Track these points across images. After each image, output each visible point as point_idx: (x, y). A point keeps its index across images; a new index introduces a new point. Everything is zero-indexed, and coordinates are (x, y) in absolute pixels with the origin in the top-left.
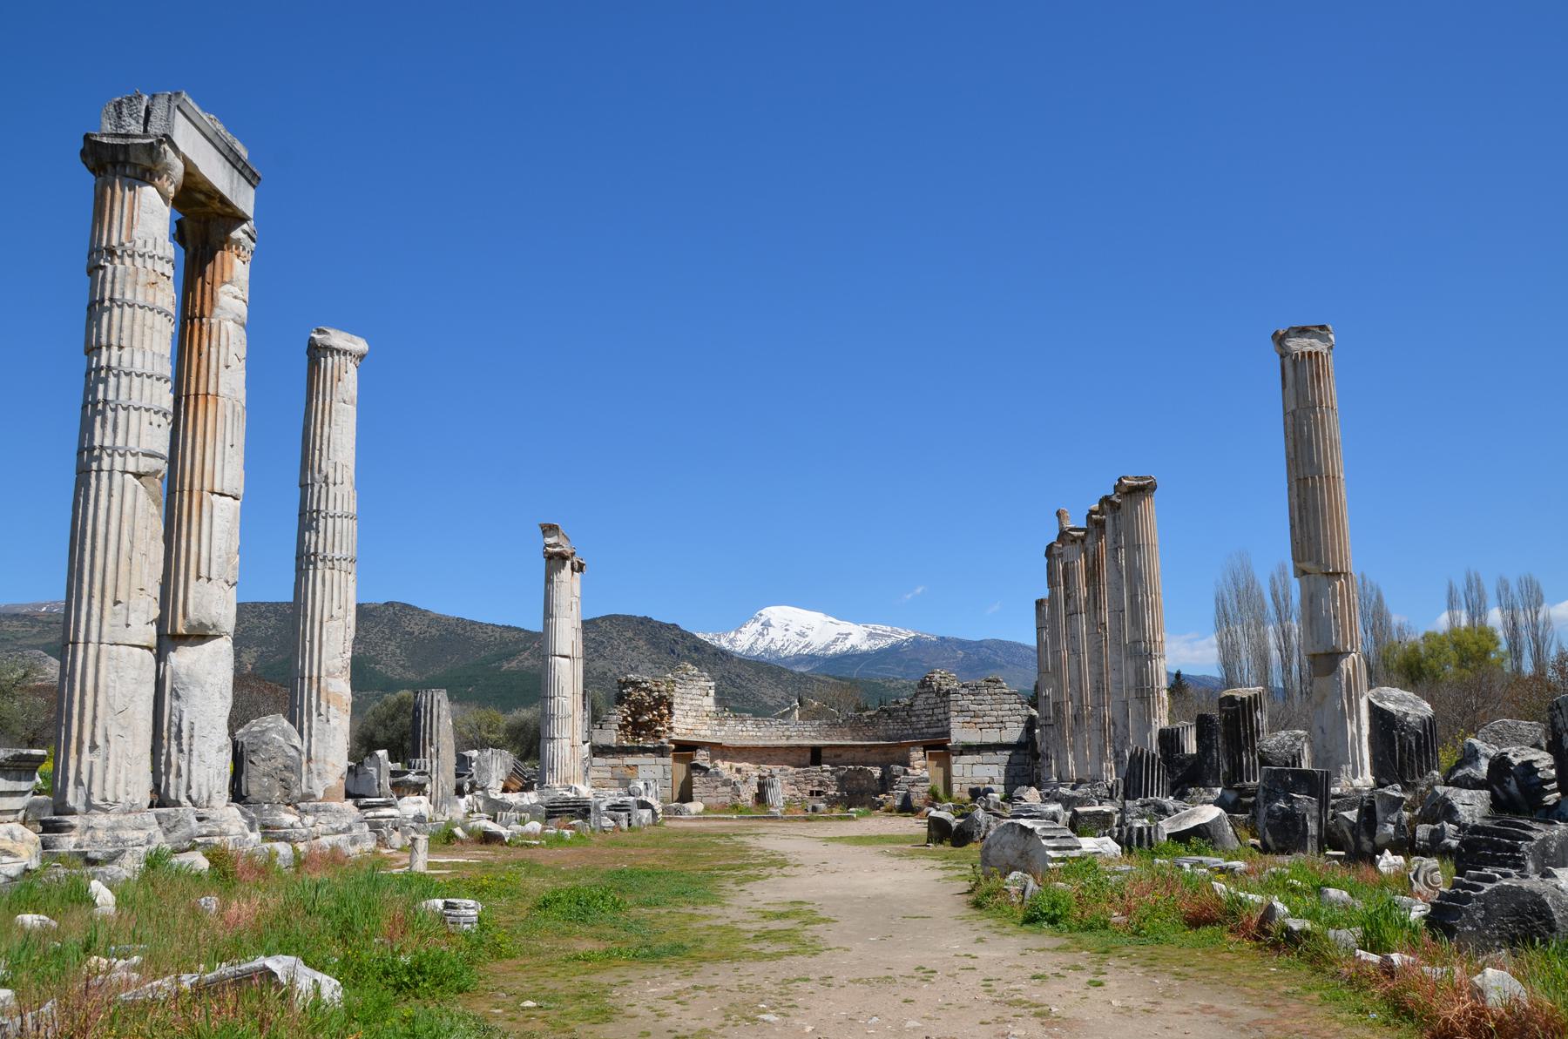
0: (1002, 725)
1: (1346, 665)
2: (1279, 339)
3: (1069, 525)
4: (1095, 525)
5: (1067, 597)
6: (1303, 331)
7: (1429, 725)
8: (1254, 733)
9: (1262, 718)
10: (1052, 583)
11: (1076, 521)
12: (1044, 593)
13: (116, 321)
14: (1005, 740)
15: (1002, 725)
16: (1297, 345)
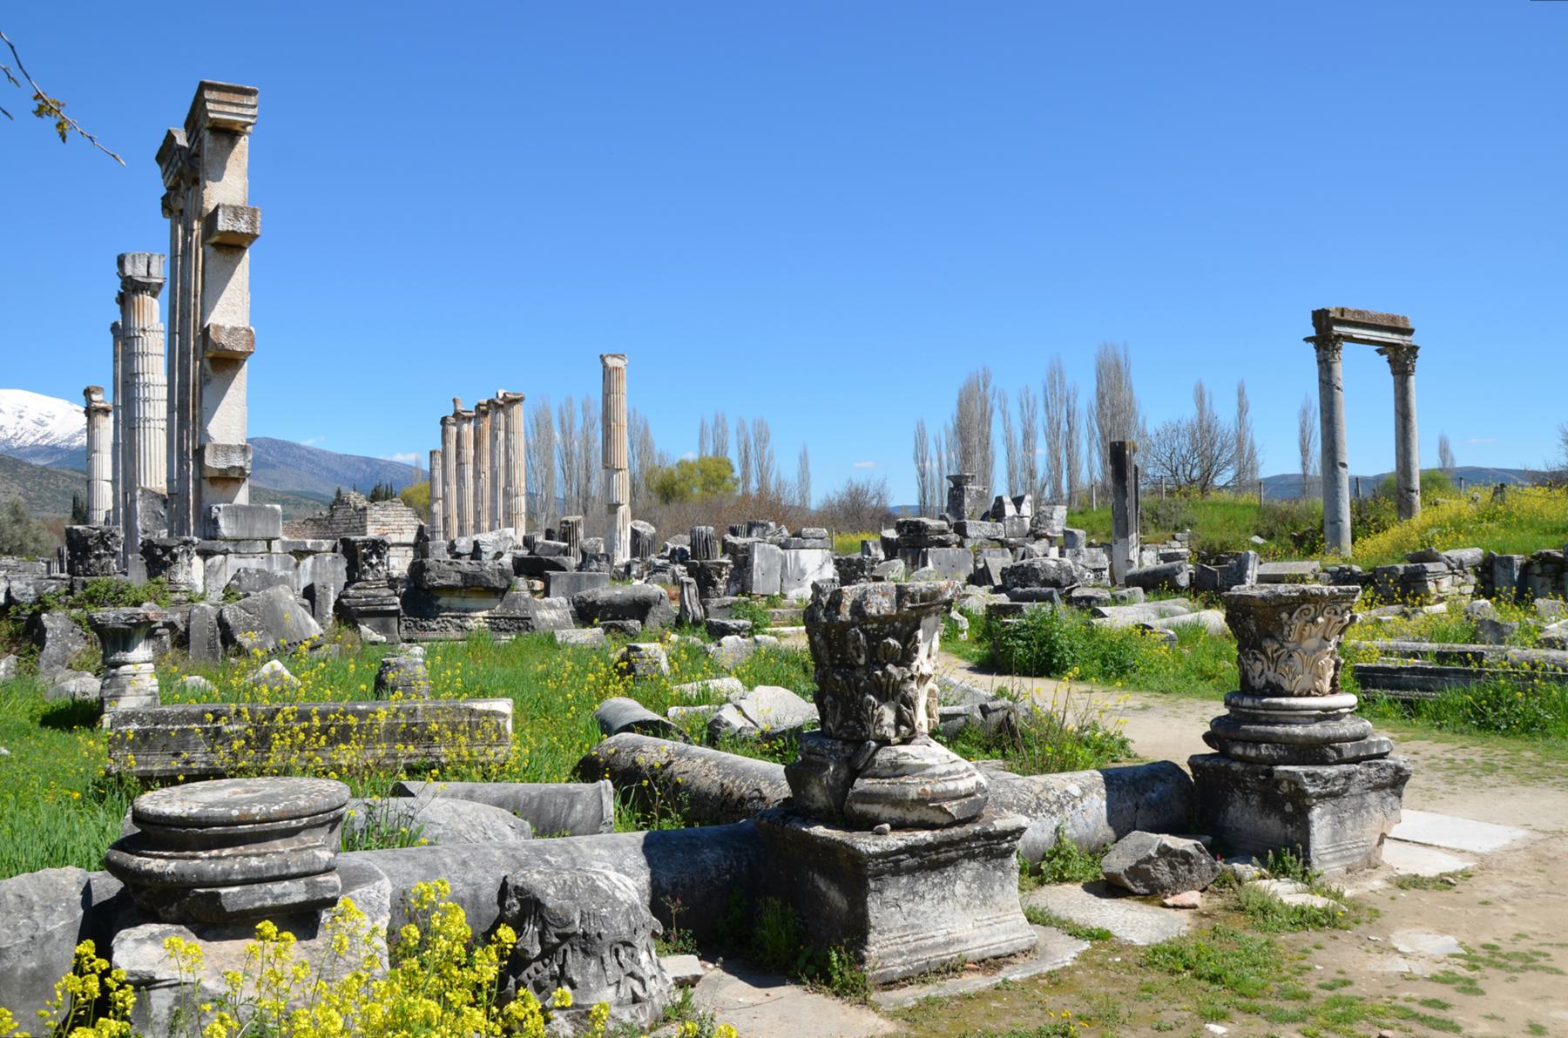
0: (401, 531)
1: (622, 509)
2: (602, 358)
3: (460, 408)
4: (481, 412)
5: (458, 455)
6: (614, 356)
7: (654, 537)
8: (577, 538)
9: (581, 531)
10: (444, 442)
11: (467, 406)
12: (439, 447)
13: (141, 364)
14: (404, 540)
15: (401, 531)
16: (611, 362)
